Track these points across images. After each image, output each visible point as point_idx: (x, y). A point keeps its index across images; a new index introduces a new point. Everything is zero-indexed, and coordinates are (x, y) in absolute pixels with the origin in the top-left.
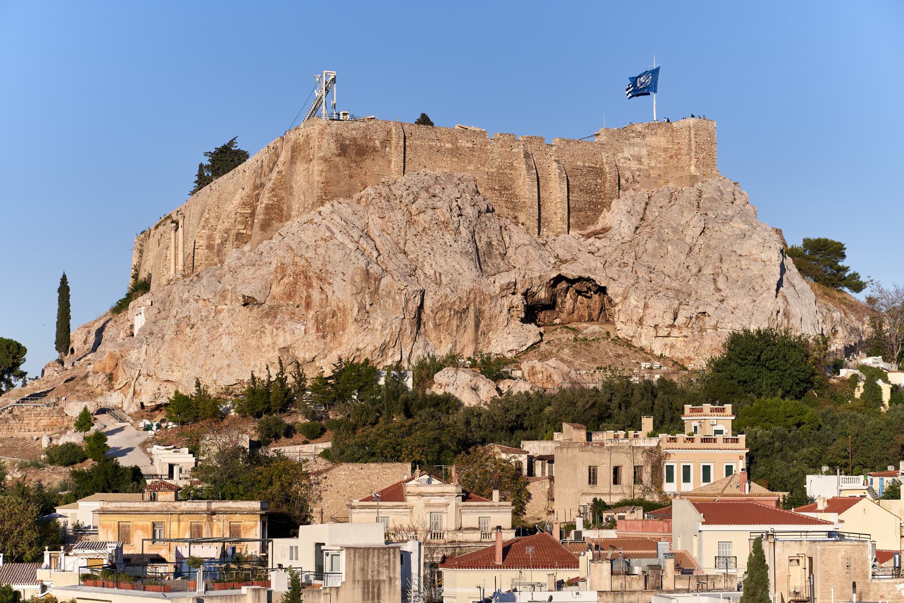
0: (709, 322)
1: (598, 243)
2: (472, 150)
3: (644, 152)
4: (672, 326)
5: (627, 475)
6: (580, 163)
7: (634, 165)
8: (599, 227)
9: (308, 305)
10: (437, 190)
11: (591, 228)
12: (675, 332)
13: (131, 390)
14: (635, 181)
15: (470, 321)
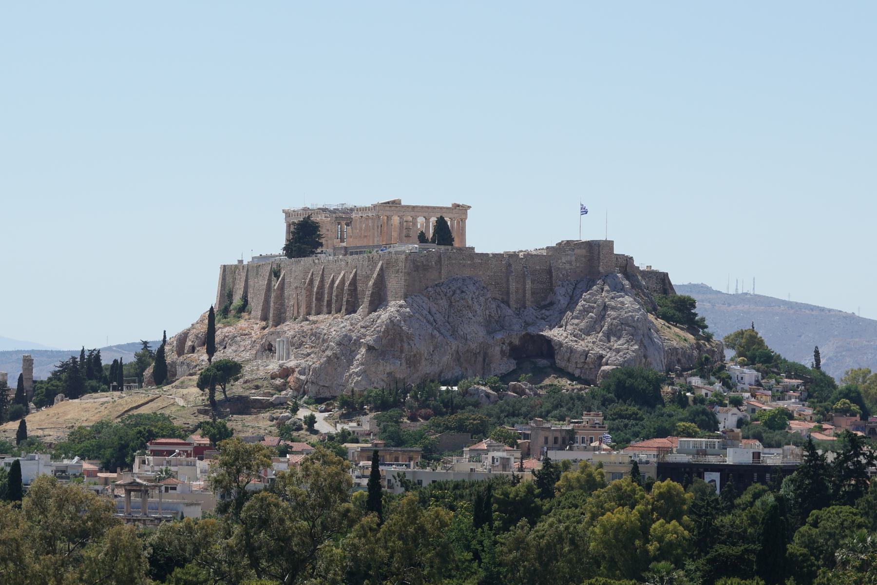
0: (604, 360)
1: (547, 313)
2: (481, 264)
3: (573, 258)
4: (585, 363)
5: (560, 440)
6: (538, 267)
7: (568, 266)
8: (547, 302)
9: (402, 351)
10: (465, 289)
11: (543, 303)
12: (586, 366)
13: (302, 390)
14: (568, 276)
15: (480, 359)
